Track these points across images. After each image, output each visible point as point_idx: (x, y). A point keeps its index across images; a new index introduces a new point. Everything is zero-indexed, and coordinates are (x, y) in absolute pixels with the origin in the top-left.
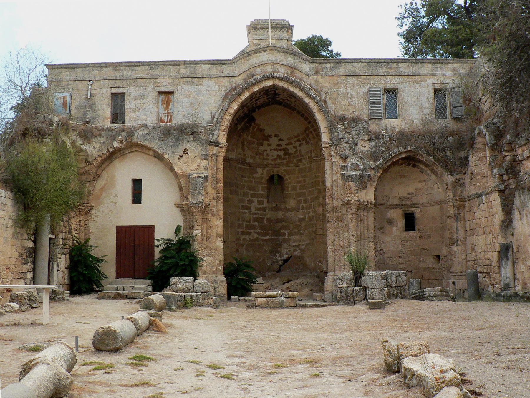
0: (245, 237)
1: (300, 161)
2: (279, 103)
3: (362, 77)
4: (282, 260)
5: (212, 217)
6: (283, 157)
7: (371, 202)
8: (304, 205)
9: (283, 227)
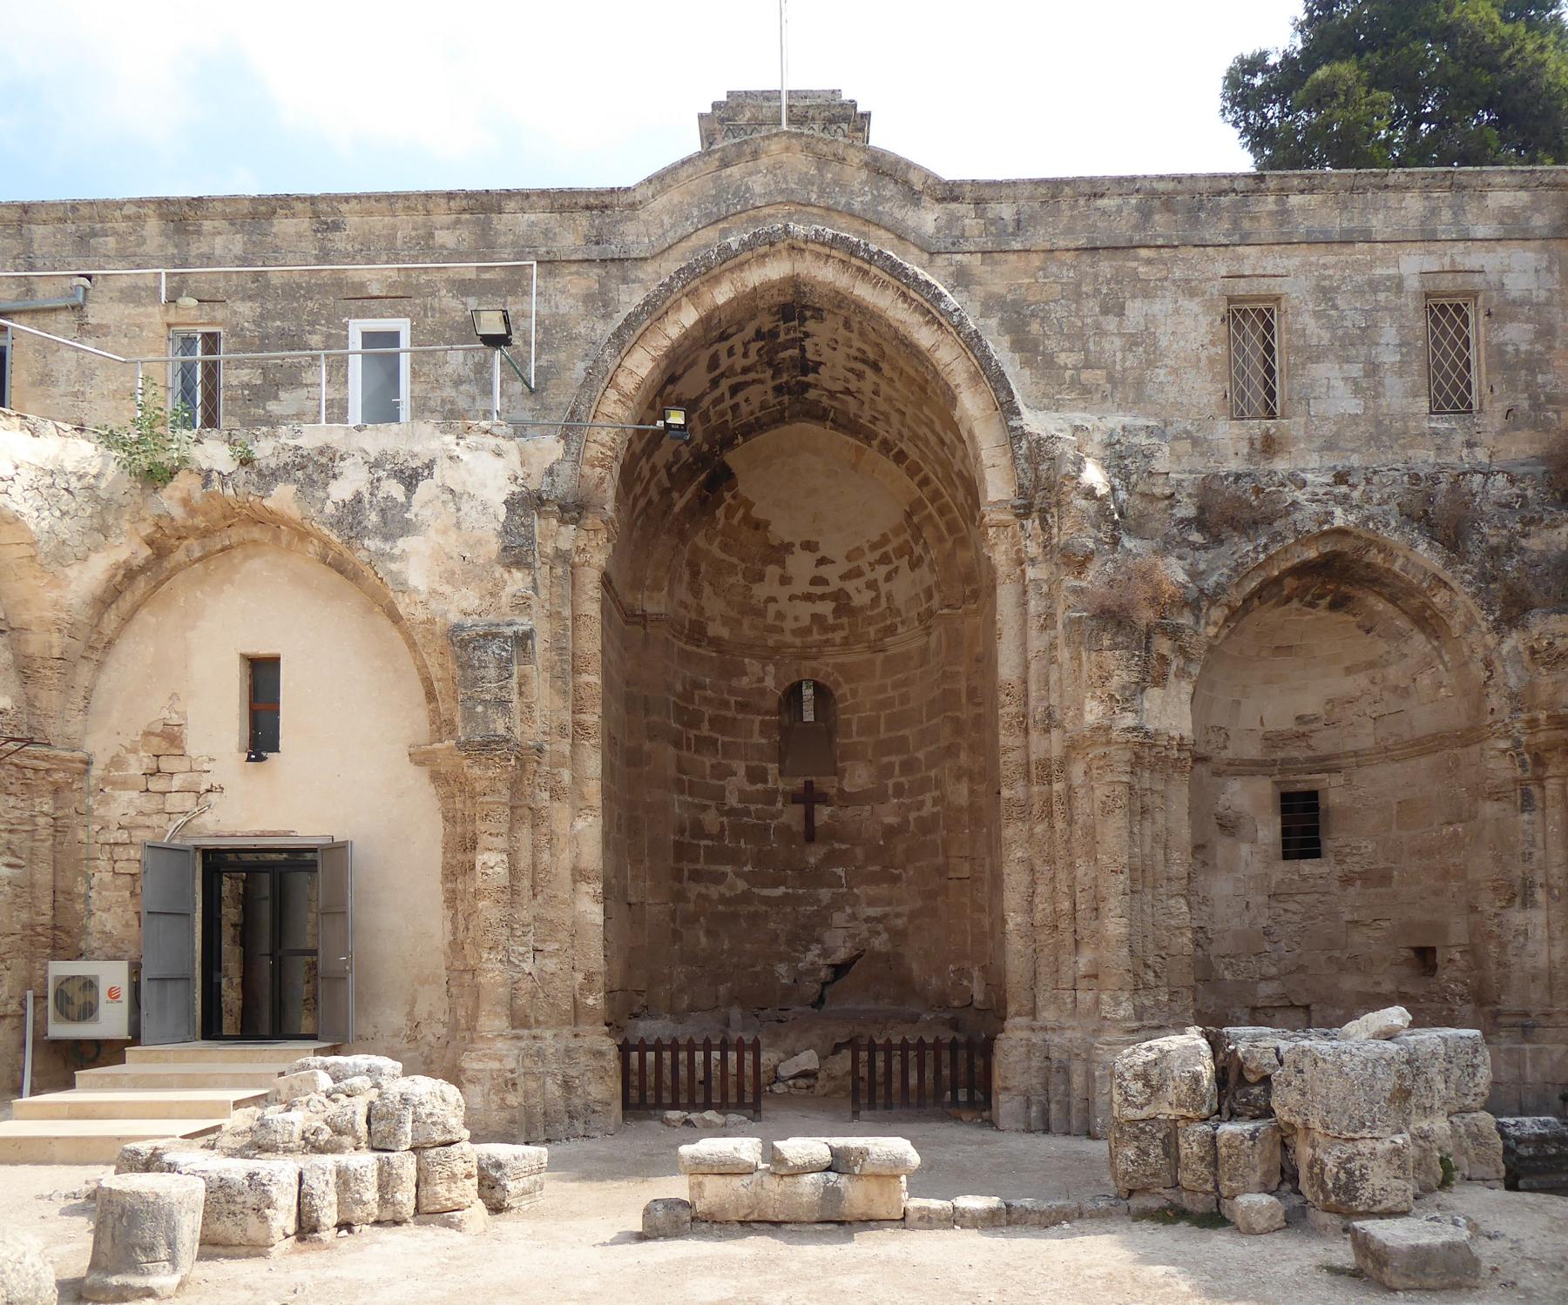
2: (818, 415)
5: (556, 804)
7: (1182, 738)
9: (833, 858)
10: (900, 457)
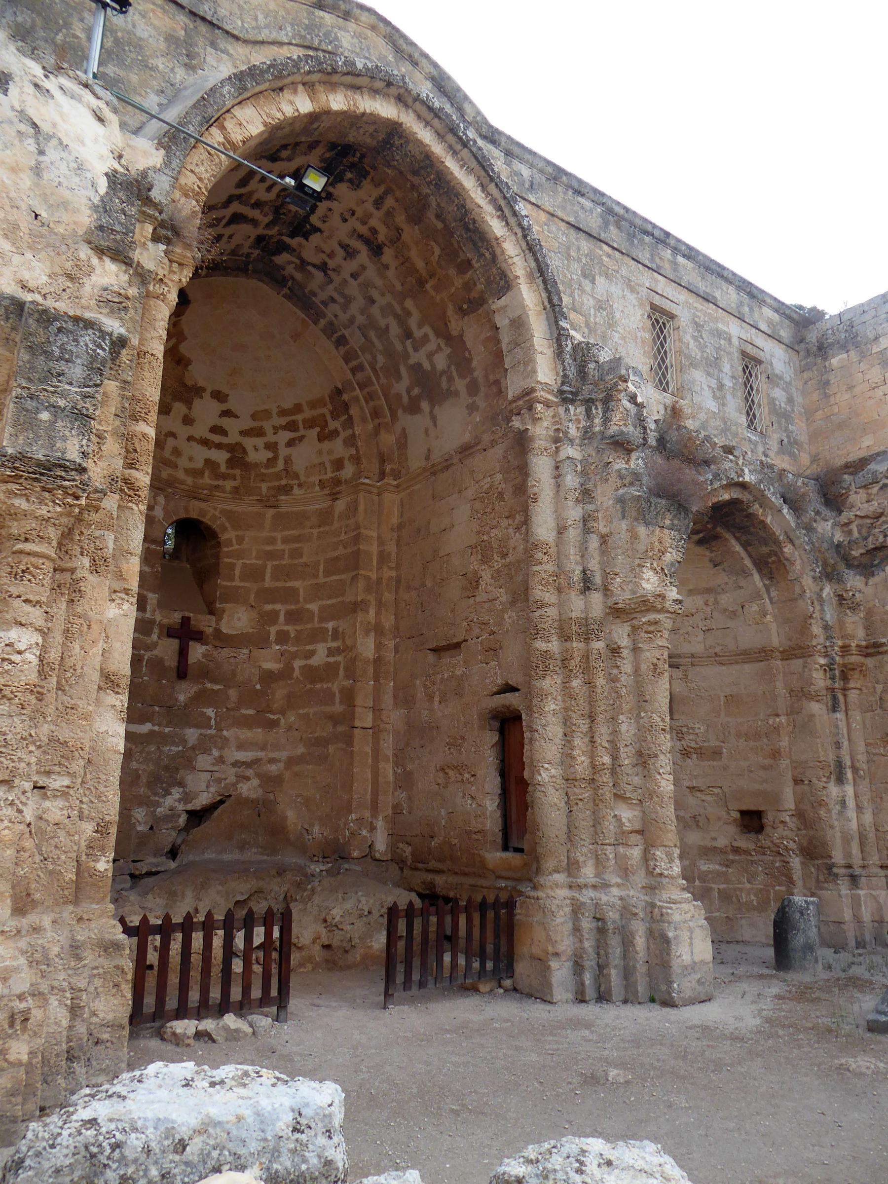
1: (286, 490)
2: (277, 279)
3: (605, 247)
4: (188, 812)
6: (223, 468)
9: (203, 698)
10: (341, 341)
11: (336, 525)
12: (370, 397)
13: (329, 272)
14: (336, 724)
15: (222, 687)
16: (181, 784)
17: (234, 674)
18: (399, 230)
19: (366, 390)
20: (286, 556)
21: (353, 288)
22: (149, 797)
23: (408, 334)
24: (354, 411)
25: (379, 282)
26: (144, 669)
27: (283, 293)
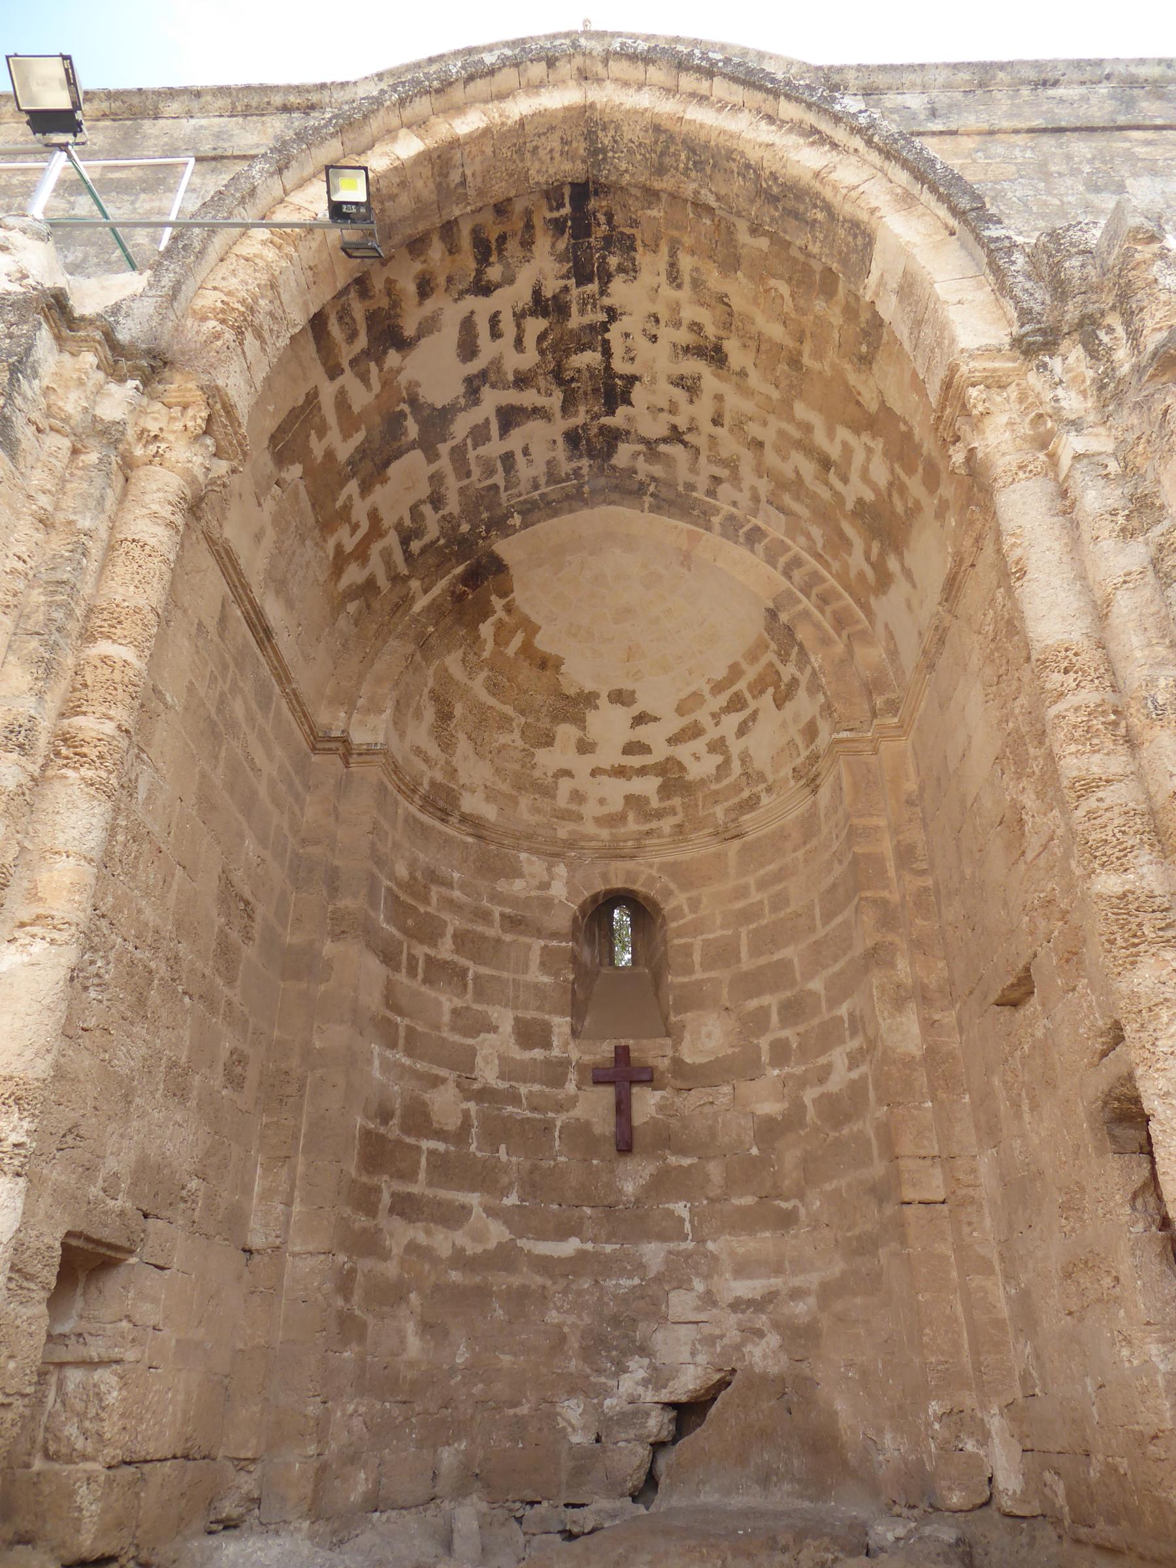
0: (422, 1239)
1: (752, 803)
8: (787, 1033)
10: (754, 536)
11: (825, 830)
12: (824, 600)
13: (686, 438)
14: (881, 1202)
15: (695, 1160)
16: (643, 1350)
17: (713, 1135)
18: (722, 299)
19: (814, 591)
20: (767, 909)
21: (730, 445)
22: (588, 1377)
23: (826, 463)
24: (803, 634)
25: (748, 406)
26: (557, 1143)
27: (647, 505)
